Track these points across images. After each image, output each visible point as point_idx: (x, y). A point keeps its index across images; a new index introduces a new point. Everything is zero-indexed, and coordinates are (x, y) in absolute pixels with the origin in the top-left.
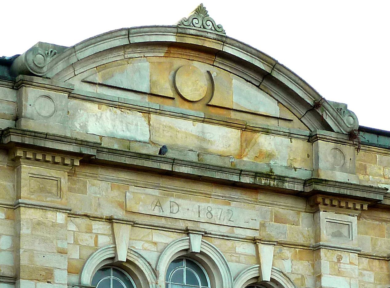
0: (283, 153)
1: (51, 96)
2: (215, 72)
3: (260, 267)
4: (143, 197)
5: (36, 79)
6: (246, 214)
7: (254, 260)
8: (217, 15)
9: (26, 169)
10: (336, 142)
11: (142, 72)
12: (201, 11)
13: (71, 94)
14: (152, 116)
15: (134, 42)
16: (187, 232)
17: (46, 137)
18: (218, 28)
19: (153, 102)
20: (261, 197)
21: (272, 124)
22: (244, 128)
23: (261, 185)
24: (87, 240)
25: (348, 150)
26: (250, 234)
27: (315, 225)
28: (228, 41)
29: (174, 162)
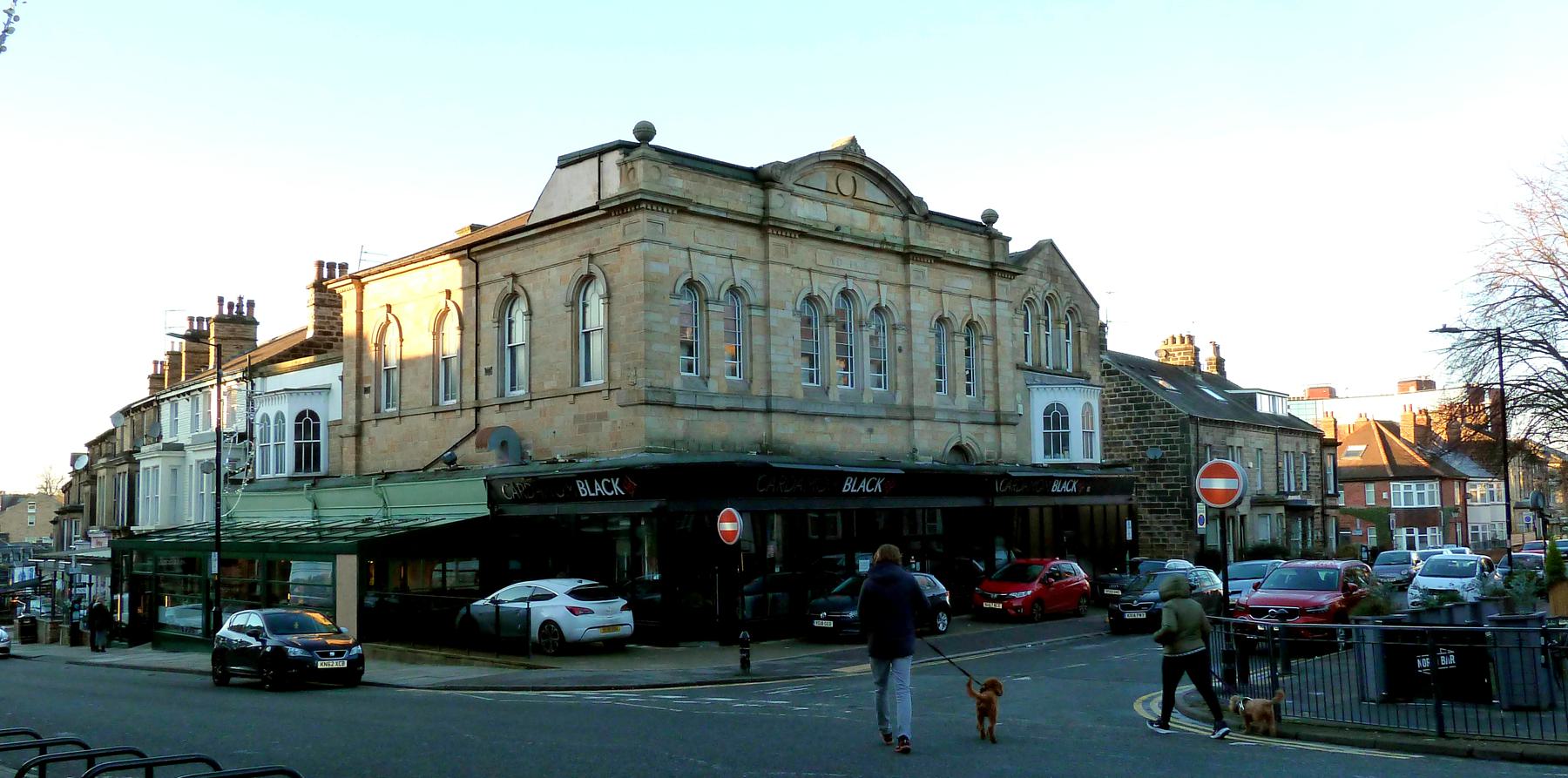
0: (889, 227)
4: (824, 255)
6: (872, 265)
8: (862, 144)
9: (772, 240)
11: (823, 179)
12: (854, 140)
13: (791, 192)
15: (820, 160)
17: (786, 222)
19: (829, 196)
21: (883, 209)
22: (872, 212)
23: (880, 247)
24: (798, 283)
25: (923, 225)
27: (907, 272)
29: (843, 235)
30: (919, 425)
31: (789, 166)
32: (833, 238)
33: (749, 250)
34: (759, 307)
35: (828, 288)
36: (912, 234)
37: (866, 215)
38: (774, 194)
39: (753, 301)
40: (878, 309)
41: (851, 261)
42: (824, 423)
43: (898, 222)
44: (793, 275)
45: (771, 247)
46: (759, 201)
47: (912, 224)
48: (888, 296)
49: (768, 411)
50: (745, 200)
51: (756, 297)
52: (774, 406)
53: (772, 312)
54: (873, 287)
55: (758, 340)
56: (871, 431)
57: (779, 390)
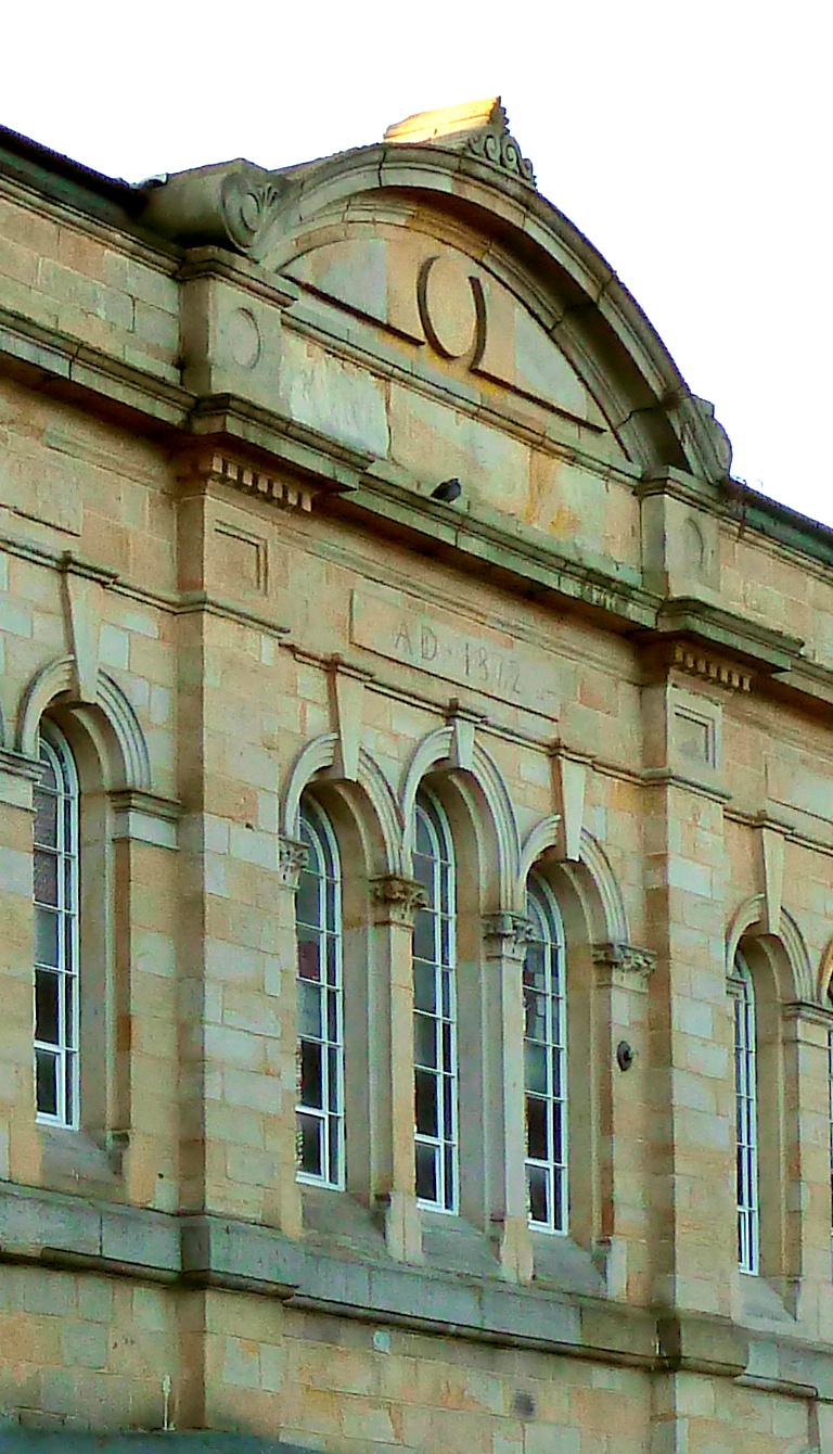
0: (583, 511)
1: (256, 311)
2: (488, 285)
3: (562, 821)
4: (380, 605)
5: (241, 264)
7: (545, 802)
9: (217, 507)
10: (693, 502)
11: (382, 261)
12: (498, 115)
14: (394, 387)
16: (451, 712)
18: (524, 168)
19: (392, 346)
20: (569, 636)
21: (567, 433)
22: (538, 443)
25: (709, 523)
26: (549, 733)
28: (539, 206)
29: (463, 524)
30: (691, 1396)
31: (283, 187)
32: (416, 533)
33: (122, 539)
34: (158, 806)
35: (385, 745)
36: (677, 556)
37: (518, 452)
38: (224, 298)
39: (134, 776)
40: (552, 874)
41: (472, 644)
42: (374, 1360)
43: (620, 499)
44: (293, 675)
45: (214, 548)
46: (165, 334)
47: (675, 512)
48: (594, 818)
49: (191, 1281)
50: (108, 302)
51: (148, 761)
52: (222, 1256)
53: (215, 830)
54: (534, 767)
55: (152, 954)
56: (525, 1407)
57: (230, 1190)
